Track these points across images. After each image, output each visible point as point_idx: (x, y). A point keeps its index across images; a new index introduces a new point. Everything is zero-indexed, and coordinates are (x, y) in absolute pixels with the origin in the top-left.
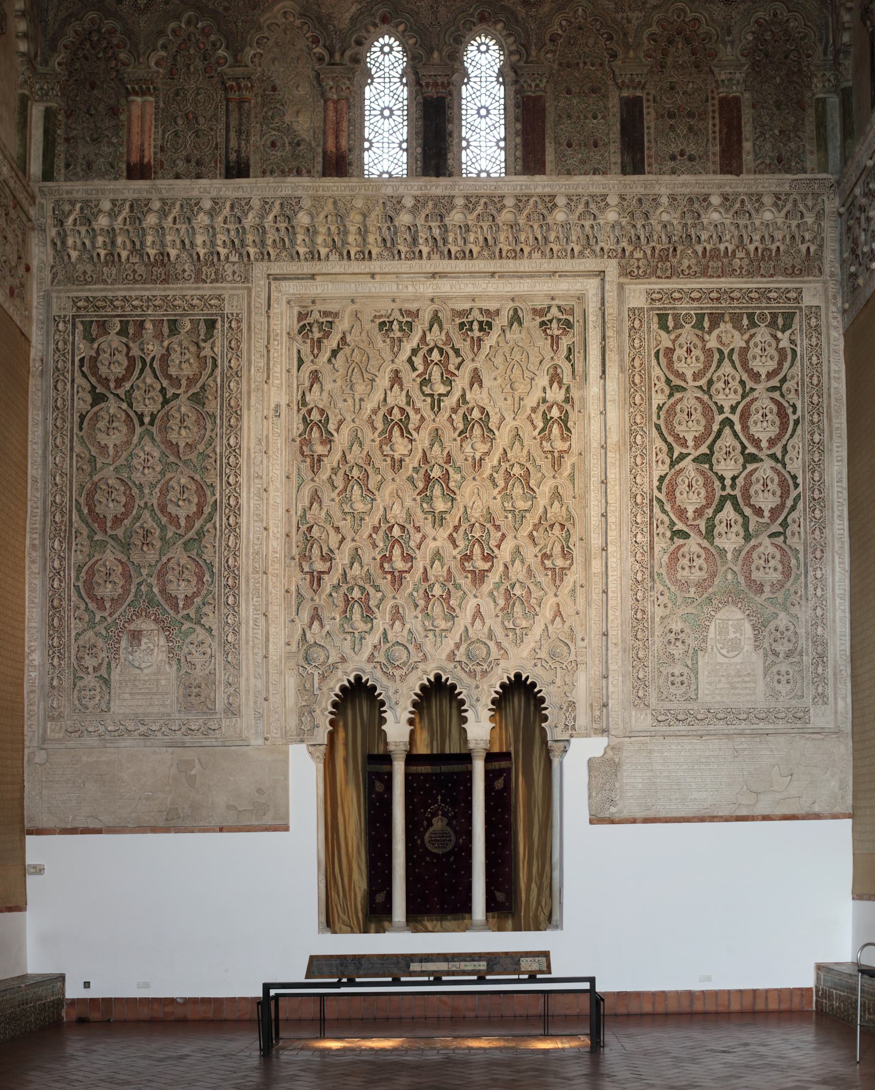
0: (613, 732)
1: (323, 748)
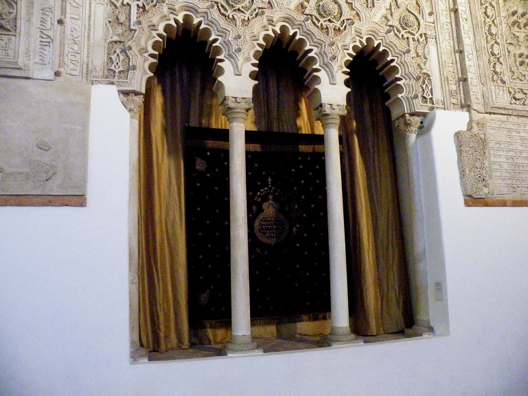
0: (475, 107)
1: (140, 100)
